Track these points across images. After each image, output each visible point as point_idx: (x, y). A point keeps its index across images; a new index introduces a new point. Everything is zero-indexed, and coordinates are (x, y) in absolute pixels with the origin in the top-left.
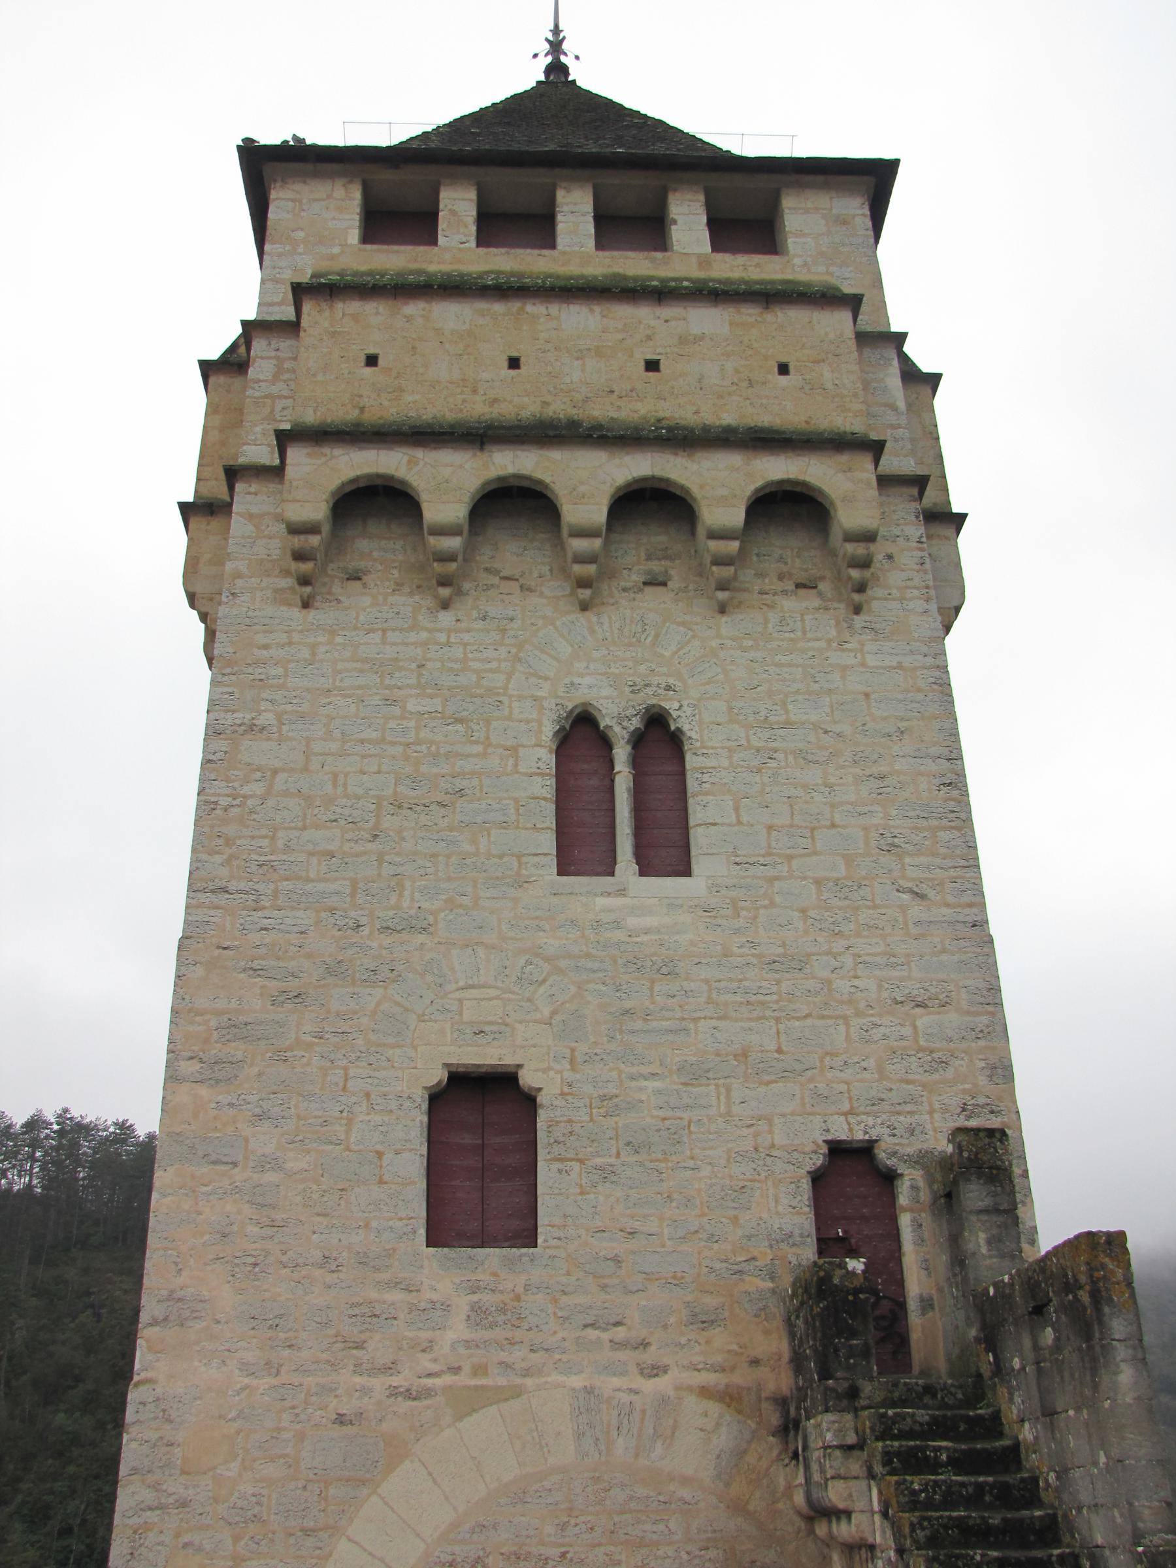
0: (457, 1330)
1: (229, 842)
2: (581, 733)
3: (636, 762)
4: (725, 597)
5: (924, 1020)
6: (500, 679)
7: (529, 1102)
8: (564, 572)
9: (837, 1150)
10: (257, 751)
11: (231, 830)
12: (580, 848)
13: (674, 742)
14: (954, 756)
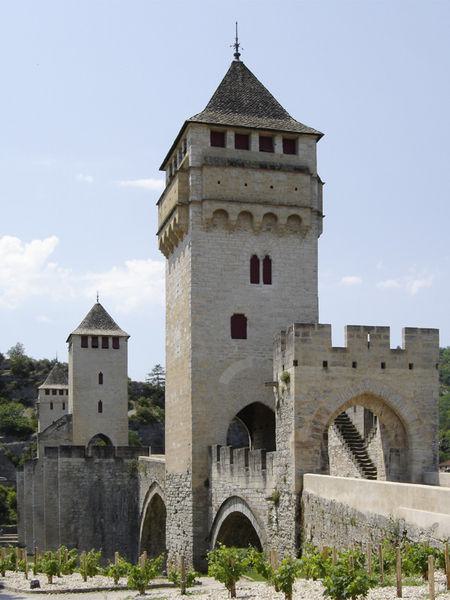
0: (237, 350)
2: (254, 260)
4: (280, 234)
5: (307, 310)
7: (246, 319)
8: (253, 228)
12: (254, 280)
13: (270, 261)
14: (316, 266)
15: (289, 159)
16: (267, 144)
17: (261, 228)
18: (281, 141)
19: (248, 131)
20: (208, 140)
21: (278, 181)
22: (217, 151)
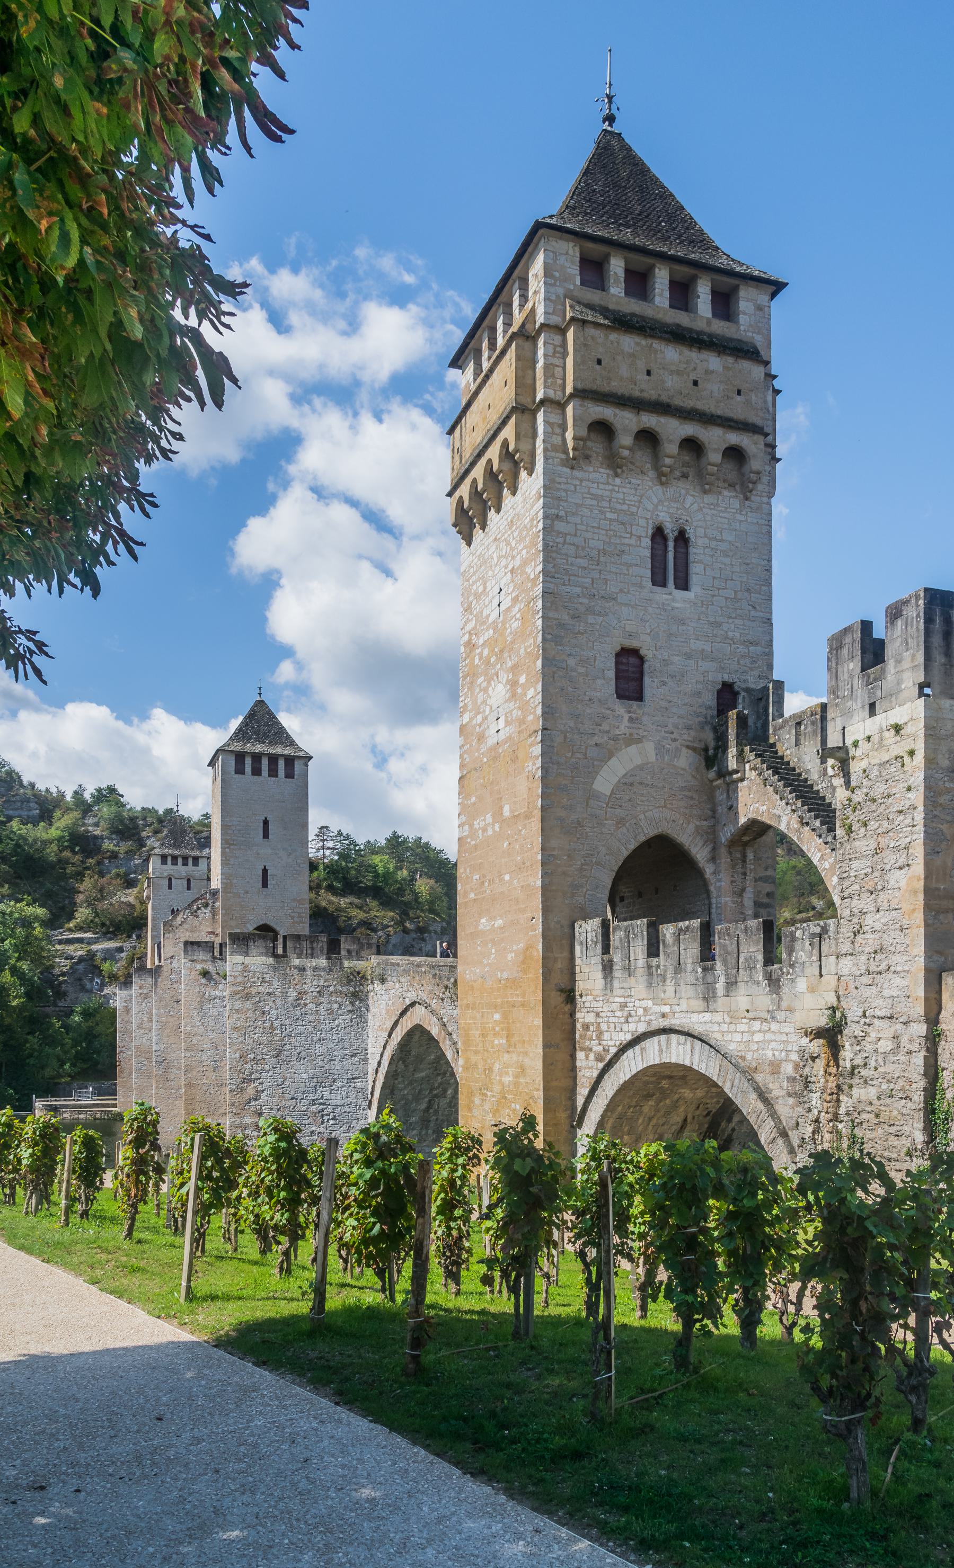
1: (554, 559)
2: (659, 533)
3: (675, 547)
6: (634, 509)
10: (560, 526)
11: (554, 555)
19: (650, 261)
20: (574, 270)
21: (708, 372)
22: (594, 296)
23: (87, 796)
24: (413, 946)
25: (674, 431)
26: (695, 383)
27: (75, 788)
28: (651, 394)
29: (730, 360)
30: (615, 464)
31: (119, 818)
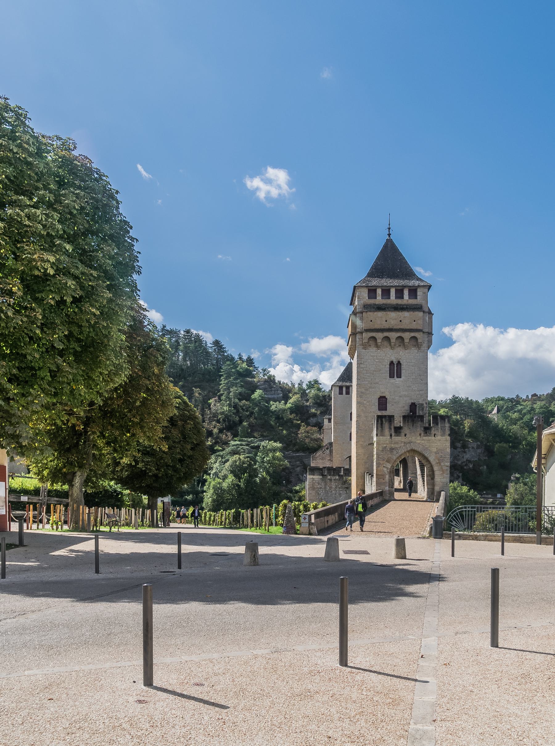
2: (392, 363)
8: (390, 345)
9: (412, 403)
10: (362, 366)
12: (391, 376)
13: (401, 364)
15: (412, 302)
16: (400, 293)
17: (395, 345)
18: (407, 292)
23: (304, 386)
24: (458, 456)
25: (393, 336)
26: (401, 321)
27: (299, 382)
28: (387, 327)
29: (412, 312)
30: (377, 347)
31: (317, 397)
